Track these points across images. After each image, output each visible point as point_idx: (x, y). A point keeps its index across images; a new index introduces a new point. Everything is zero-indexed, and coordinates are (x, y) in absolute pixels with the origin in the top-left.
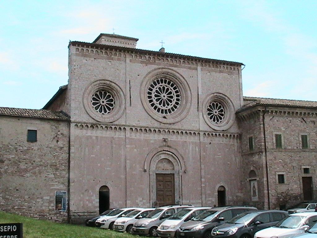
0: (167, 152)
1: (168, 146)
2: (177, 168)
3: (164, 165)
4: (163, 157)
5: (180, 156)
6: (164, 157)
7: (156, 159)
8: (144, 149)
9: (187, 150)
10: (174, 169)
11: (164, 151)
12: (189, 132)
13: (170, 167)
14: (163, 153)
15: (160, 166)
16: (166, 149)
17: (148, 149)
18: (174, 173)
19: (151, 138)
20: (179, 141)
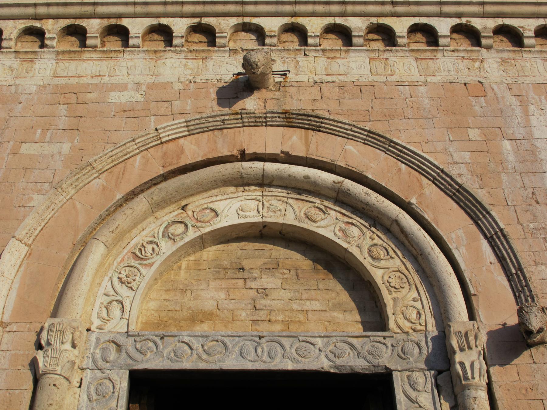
0: (271, 167)
1: (290, 119)
2: (406, 304)
3: (264, 292)
4: (236, 208)
5: (431, 190)
6: (253, 217)
7: (153, 227)
8: (25, 149)
9: (507, 145)
10: (374, 315)
11: (243, 156)
12: (492, 23)
13: (339, 315)
14: (242, 182)
15: (209, 305)
16: (272, 139)
17: (66, 148)
18: (386, 359)
19: (122, 77)
20: (399, 84)
